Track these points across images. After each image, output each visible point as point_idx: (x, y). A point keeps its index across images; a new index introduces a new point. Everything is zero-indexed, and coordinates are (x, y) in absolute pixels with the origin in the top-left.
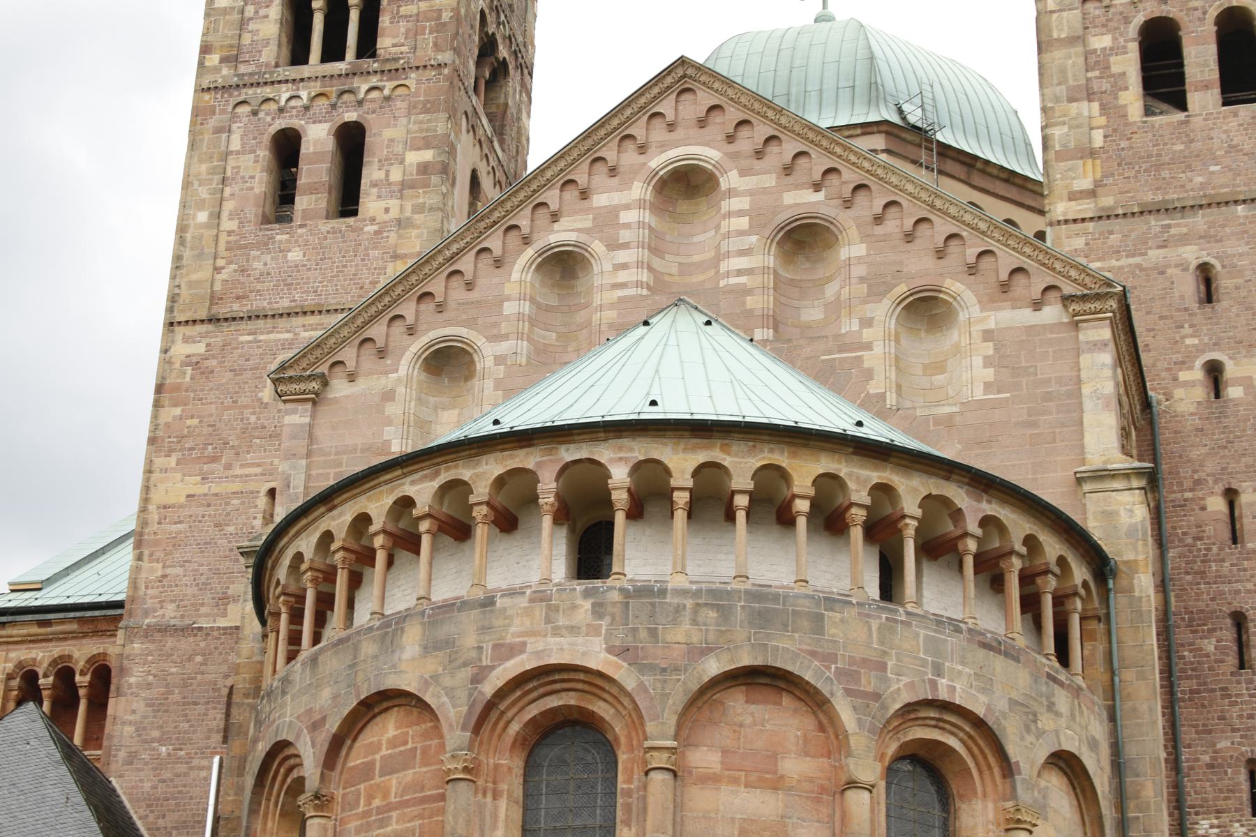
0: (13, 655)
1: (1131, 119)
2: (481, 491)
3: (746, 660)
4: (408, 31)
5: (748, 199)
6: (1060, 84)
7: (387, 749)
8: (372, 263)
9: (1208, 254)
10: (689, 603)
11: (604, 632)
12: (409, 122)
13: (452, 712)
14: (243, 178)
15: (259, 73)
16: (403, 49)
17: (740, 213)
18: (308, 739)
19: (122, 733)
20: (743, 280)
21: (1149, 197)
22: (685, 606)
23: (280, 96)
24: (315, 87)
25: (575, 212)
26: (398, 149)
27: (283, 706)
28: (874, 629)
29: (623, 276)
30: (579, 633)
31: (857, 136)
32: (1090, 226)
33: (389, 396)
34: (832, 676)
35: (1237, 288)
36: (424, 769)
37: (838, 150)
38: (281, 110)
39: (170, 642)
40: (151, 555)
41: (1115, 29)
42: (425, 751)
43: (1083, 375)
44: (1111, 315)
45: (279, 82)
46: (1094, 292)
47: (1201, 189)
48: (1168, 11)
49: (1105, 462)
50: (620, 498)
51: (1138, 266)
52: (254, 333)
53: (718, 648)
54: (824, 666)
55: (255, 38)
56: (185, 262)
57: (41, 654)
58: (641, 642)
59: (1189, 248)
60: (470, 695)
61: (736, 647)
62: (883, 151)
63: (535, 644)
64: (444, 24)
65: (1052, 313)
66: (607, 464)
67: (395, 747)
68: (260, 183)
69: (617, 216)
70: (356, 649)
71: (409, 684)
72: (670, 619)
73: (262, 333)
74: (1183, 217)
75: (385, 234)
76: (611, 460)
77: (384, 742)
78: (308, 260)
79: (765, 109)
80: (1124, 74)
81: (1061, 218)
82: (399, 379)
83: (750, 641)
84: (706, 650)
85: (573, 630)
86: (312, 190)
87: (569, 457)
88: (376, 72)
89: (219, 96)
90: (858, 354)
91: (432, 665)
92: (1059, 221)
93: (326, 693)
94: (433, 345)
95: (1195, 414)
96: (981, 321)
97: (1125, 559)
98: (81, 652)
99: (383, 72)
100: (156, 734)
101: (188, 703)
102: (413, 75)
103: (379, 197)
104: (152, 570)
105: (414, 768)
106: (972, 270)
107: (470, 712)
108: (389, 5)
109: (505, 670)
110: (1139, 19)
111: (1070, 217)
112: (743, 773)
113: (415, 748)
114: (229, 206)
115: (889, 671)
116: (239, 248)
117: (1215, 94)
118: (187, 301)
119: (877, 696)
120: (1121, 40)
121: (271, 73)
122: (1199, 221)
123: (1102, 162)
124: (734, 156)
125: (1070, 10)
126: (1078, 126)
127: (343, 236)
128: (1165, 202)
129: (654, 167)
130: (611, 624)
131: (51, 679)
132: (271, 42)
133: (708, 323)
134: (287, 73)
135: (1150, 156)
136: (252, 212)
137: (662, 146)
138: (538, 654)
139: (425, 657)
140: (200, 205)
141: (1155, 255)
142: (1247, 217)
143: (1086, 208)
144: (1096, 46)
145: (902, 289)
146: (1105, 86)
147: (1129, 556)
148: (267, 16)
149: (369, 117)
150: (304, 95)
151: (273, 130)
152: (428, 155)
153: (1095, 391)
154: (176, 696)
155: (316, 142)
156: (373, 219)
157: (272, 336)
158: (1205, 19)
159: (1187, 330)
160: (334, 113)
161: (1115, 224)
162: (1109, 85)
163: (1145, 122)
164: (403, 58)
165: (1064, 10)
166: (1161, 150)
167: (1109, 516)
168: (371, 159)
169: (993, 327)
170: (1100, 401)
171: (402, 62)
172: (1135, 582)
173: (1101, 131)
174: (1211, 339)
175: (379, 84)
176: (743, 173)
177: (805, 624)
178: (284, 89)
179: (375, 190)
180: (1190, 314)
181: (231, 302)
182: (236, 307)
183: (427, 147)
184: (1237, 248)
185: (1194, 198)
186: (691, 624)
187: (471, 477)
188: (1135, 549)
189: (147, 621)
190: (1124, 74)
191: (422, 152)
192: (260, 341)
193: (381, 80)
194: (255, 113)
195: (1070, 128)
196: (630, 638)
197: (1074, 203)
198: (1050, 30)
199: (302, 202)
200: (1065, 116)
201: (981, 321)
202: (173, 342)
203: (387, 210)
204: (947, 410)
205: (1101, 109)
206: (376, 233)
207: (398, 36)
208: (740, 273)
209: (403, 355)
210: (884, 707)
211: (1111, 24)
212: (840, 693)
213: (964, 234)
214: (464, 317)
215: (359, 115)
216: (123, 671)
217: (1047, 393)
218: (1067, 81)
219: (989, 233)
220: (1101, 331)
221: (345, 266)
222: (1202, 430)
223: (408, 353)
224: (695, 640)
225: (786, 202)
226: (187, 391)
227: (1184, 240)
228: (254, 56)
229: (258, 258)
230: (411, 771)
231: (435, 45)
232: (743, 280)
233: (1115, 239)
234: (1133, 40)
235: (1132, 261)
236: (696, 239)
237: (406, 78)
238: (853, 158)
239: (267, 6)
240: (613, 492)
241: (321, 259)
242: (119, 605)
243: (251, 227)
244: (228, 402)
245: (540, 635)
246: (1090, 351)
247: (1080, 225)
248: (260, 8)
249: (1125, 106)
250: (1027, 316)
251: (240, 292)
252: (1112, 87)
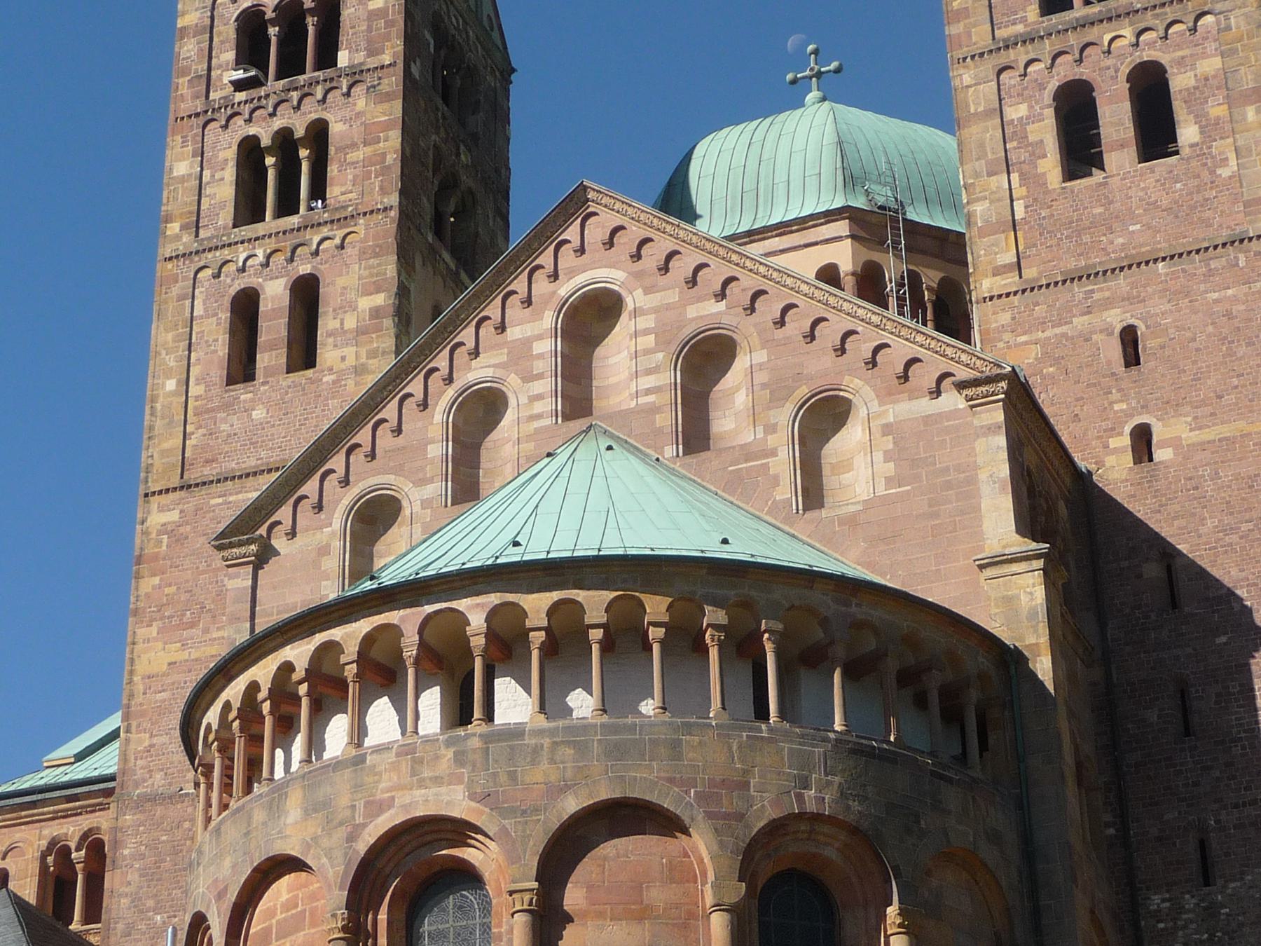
0: (46, 832)
1: (1050, 188)
2: (351, 651)
3: (604, 793)
4: (355, 177)
5: (653, 316)
6: (978, 159)
7: (281, 913)
8: (332, 414)
9: (1132, 316)
10: (547, 742)
11: (466, 780)
12: (360, 269)
13: (331, 873)
14: (207, 342)
15: (218, 236)
16: (350, 196)
17: (646, 332)
18: (215, 908)
19: (119, 905)
20: (651, 398)
21: (1072, 263)
22: (542, 745)
23: (238, 257)
24: (269, 244)
25: (492, 348)
26: (352, 295)
27: (198, 877)
28: (735, 748)
29: (539, 407)
30: (443, 783)
31: (822, 224)
32: (1015, 300)
33: (324, 551)
34: (692, 801)
35: (1163, 347)
36: (313, 931)
37: (735, 257)
39: (159, 811)
40: (138, 726)
41: (1031, 97)
42: (312, 914)
43: (980, 460)
44: (1003, 396)
45: (236, 243)
46: (983, 375)
47: (1122, 251)
48: (1082, 74)
49: (1004, 547)
50: (478, 642)
51: (1064, 335)
52: (225, 495)
53: (575, 784)
54: (682, 791)
55: (212, 202)
56: (156, 432)
57: (72, 829)
58: (501, 787)
59: (1113, 312)
60: (346, 854)
61: (594, 782)
62: (847, 237)
63: (403, 798)
64: (389, 167)
65: (952, 400)
66: (465, 612)
67: (288, 910)
68: (223, 345)
69: (531, 348)
70: (250, 818)
71: (293, 849)
72: (529, 759)
73: (231, 494)
74: (1105, 281)
75: (343, 383)
76: (470, 608)
77: (279, 907)
78: (271, 417)
79: (664, 225)
80: (1042, 141)
81: (986, 295)
82: (333, 533)
83: (607, 774)
84: (564, 788)
85: (437, 780)
86: (272, 347)
87: (429, 609)
88: (326, 222)
89: (181, 263)
90: (764, 461)
91: (313, 827)
92: (985, 298)
93: (227, 862)
94: (364, 496)
95: (1127, 480)
96: (880, 415)
97: (1027, 643)
98: (71, 830)
99: (332, 222)
100: (151, 903)
101: (180, 870)
102: (361, 221)
103: (335, 346)
104: (140, 741)
105: (304, 930)
106: (872, 363)
107: (345, 872)
108: (336, 154)
109: (376, 826)
110: (1054, 85)
111: (995, 293)
112: (608, 907)
113: (305, 910)
114: (194, 371)
115: (752, 790)
116: (208, 411)
117: (1132, 152)
118: (160, 471)
119: (740, 817)
120: (1037, 108)
121: (229, 235)
122: (1121, 283)
123: (1025, 233)
124: (638, 275)
125: (984, 83)
126: (999, 200)
127: (304, 389)
128: (1087, 267)
129: (563, 294)
130: (473, 771)
131: (83, 852)
132: (227, 204)
133: (610, 448)
134: (243, 233)
135: (1071, 222)
136: (218, 373)
137: (571, 272)
138: (405, 807)
139: (306, 820)
141: (1080, 322)
142: (1167, 274)
143: (1010, 281)
144: (1013, 117)
145: (803, 391)
146: (1024, 155)
147: (1031, 640)
148: (222, 179)
149: (322, 267)
150: (260, 253)
151: (233, 291)
153: (991, 476)
154: (167, 864)
155: (273, 298)
156: (331, 369)
157: (240, 496)
158: (1117, 77)
159: (1115, 395)
160: (290, 267)
161: (1037, 294)
162: (1027, 154)
163: (1064, 188)
164: (352, 205)
165: (980, 84)
166: (1081, 215)
167: (1009, 601)
168: (326, 309)
169: (892, 420)
170: (997, 485)
171: (350, 209)
172: (1038, 665)
173: (1022, 201)
174: (1139, 402)
175: (330, 234)
176: (648, 291)
177: (663, 751)
178: (241, 249)
179: (331, 340)
180: (1116, 379)
181: (203, 466)
182: (207, 471)
184: (1159, 306)
185: (1116, 260)
186: (549, 763)
187: (342, 637)
188: (1036, 631)
189: (138, 791)
190: (1042, 141)
191: (373, 296)
192: (230, 503)
193: (332, 230)
195: (990, 203)
196: (491, 784)
197: (998, 278)
198: (968, 106)
199: (264, 360)
200: (985, 190)
201: (880, 415)
202: (149, 512)
203: (343, 359)
204: (852, 508)
205: (1020, 180)
206: (334, 382)
207: (346, 184)
208: (648, 392)
209: (335, 509)
210: (748, 826)
211: (1026, 92)
212: (700, 817)
213: (860, 329)
214: (392, 464)
215: (313, 267)
216: (116, 844)
217: (947, 481)
218: (986, 154)
219: (882, 326)
220: (994, 414)
221: (305, 419)
222: (1133, 496)
223: (340, 505)
224: (553, 778)
225: (689, 316)
226: (164, 559)
227: (1108, 304)
228: (212, 220)
229: (224, 420)
230: (302, 933)
231: (381, 188)
232: (651, 398)
233: (1040, 310)
234: (1049, 106)
235: (1058, 330)
236: (612, 361)
237: (355, 225)
238: (748, 264)
239: (223, 169)
240: (471, 638)
241: (284, 415)
242: (112, 778)
243: (216, 390)
244: (203, 566)
245: (406, 789)
246: (985, 435)
247: (1004, 299)
248: (216, 172)
249: (1044, 174)
250: (926, 406)
251: (209, 456)
252: (1030, 156)
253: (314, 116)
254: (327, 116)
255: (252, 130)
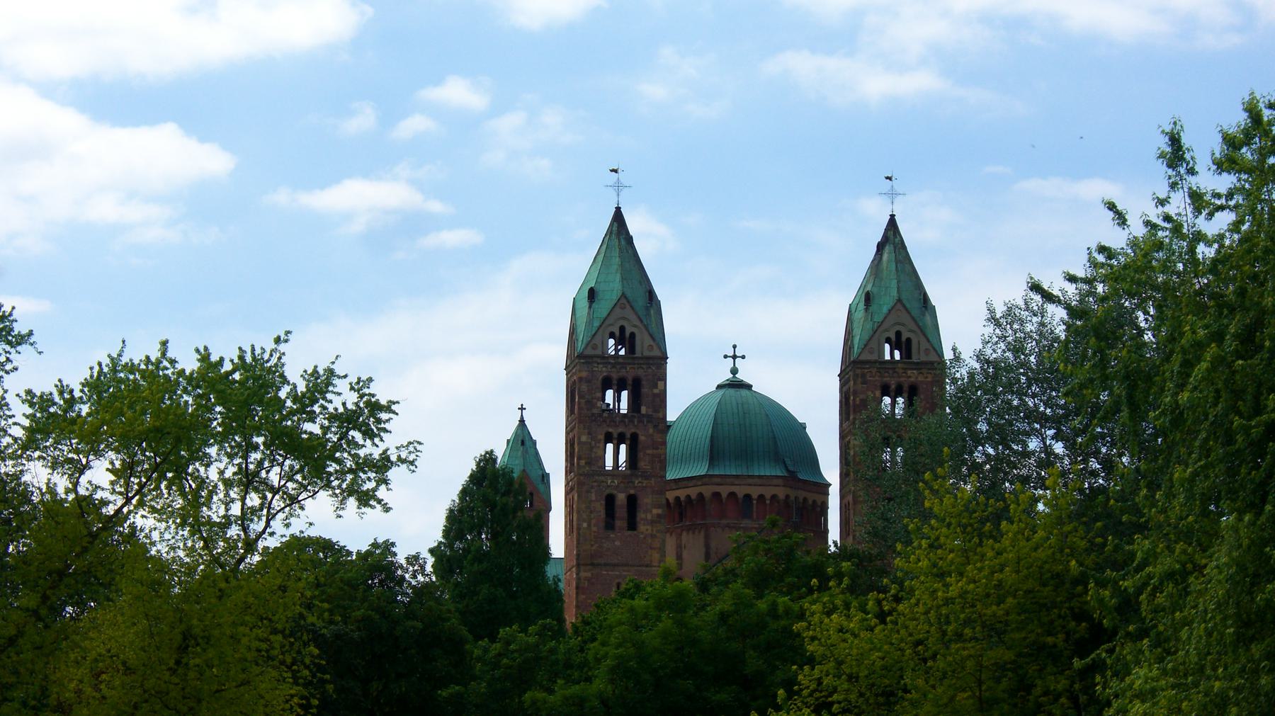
38: (608, 486)
114: (593, 522)
140: (584, 521)
151: (605, 494)
152: (660, 511)
156: (642, 533)
183: (659, 508)
194: (599, 486)
199: (618, 523)
203: (647, 530)
253: (633, 431)
254: (638, 432)
255: (610, 430)
